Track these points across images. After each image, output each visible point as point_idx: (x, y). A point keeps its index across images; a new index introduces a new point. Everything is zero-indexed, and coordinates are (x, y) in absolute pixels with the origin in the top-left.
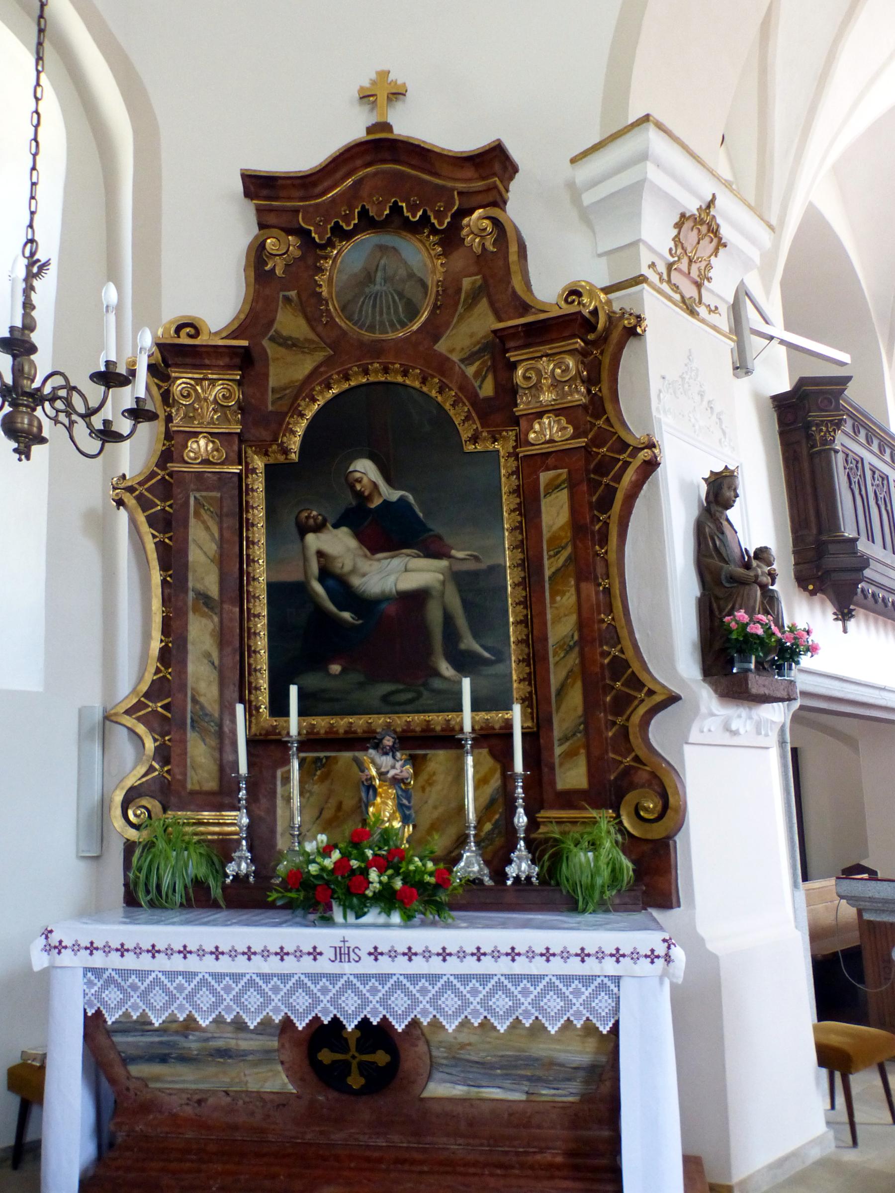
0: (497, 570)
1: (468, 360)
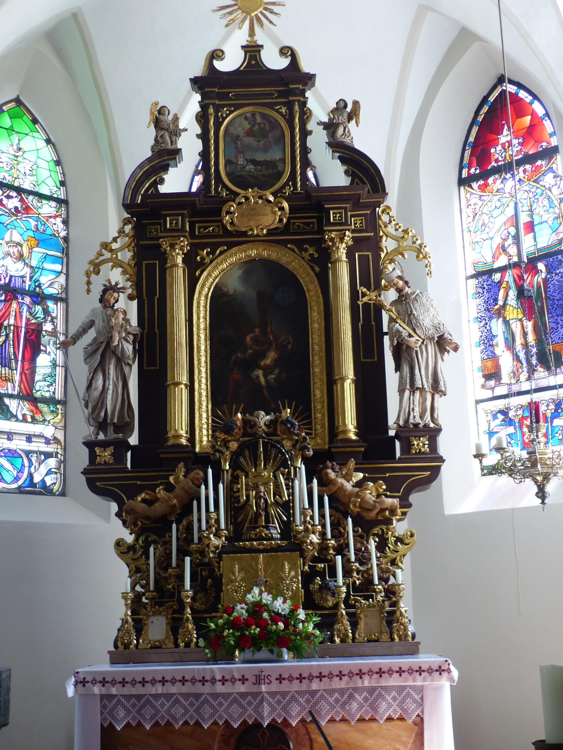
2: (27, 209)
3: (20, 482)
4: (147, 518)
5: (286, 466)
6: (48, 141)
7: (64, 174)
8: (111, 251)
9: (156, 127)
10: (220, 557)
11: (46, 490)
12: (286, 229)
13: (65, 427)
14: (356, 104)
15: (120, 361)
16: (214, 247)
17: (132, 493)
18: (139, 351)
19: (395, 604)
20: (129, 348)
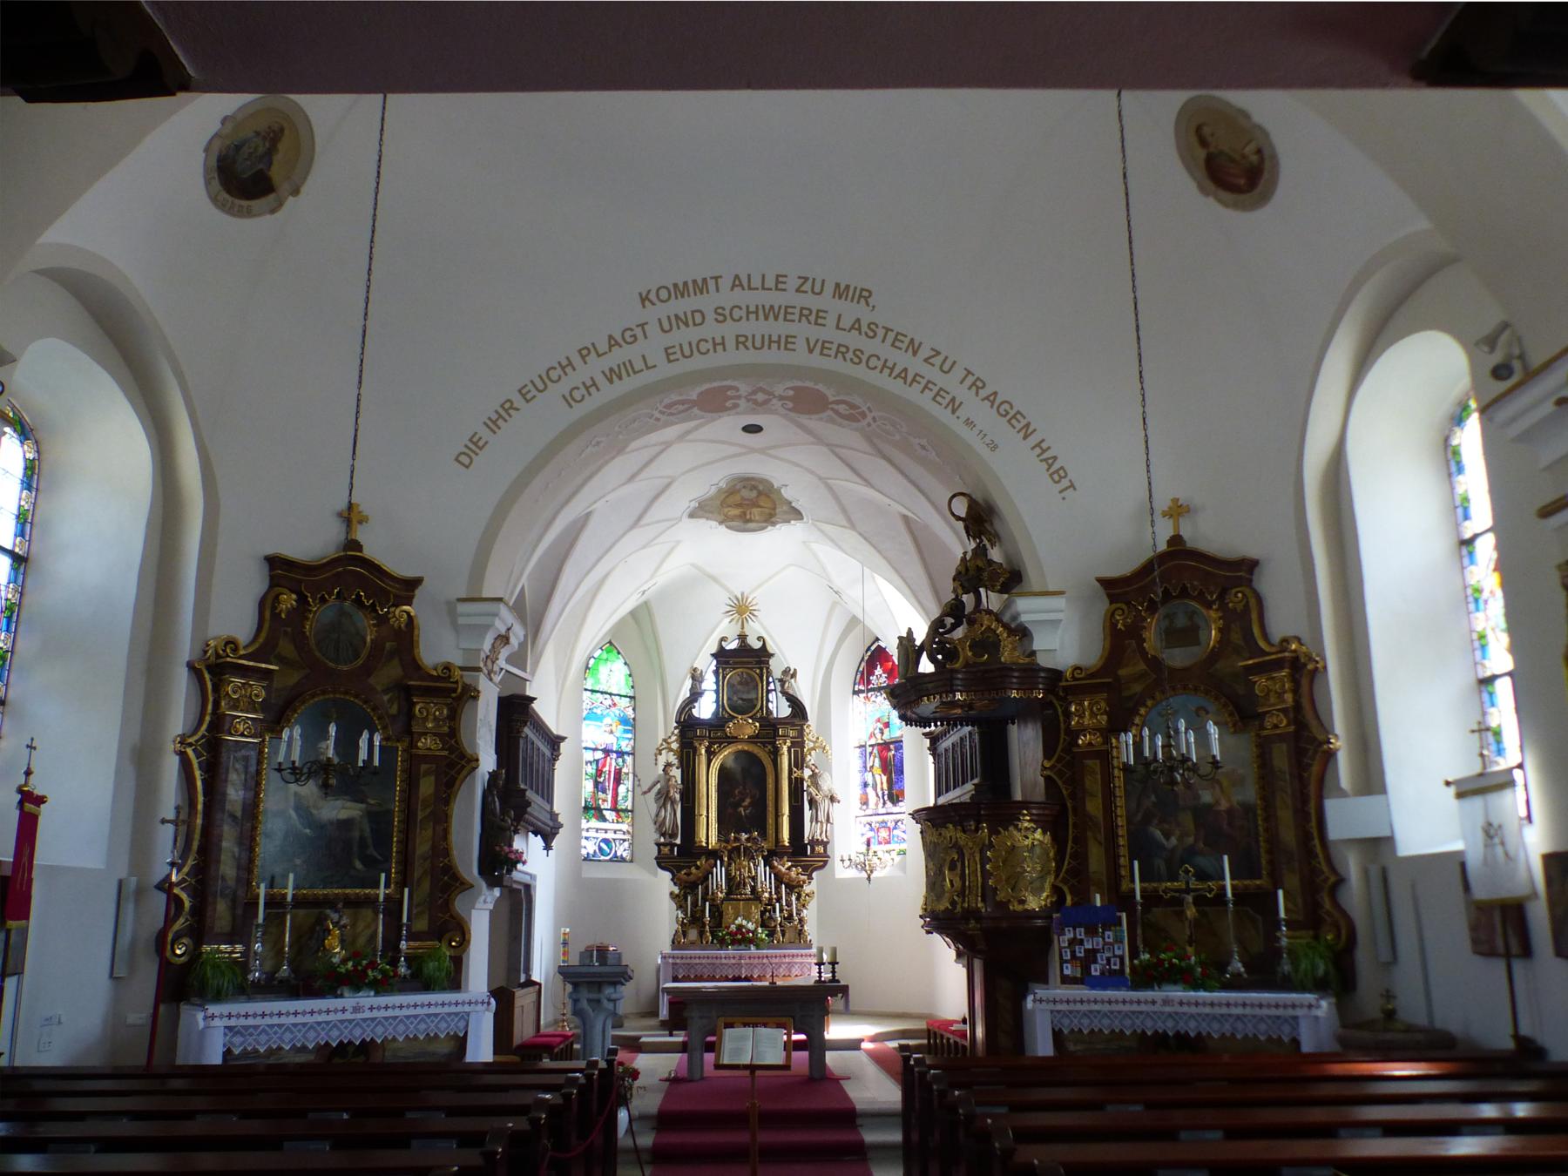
0: (390, 812)
1: (386, 691)
2: (615, 705)
3: (611, 856)
4: (686, 882)
5: (754, 859)
6: (626, 664)
7: (633, 681)
8: (668, 743)
9: (693, 678)
10: (722, 902)
11: (623, 860)
12: (757, 736)
13: (633, 825)
14: (795, 670)
15: (673, 803)
16: (721, 744)
17: (679, 869)
18: (681, 799)
19: (802, 926)
20: (678, 797)
